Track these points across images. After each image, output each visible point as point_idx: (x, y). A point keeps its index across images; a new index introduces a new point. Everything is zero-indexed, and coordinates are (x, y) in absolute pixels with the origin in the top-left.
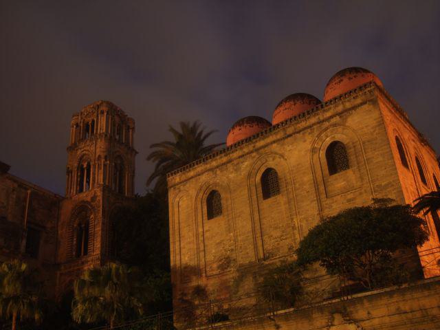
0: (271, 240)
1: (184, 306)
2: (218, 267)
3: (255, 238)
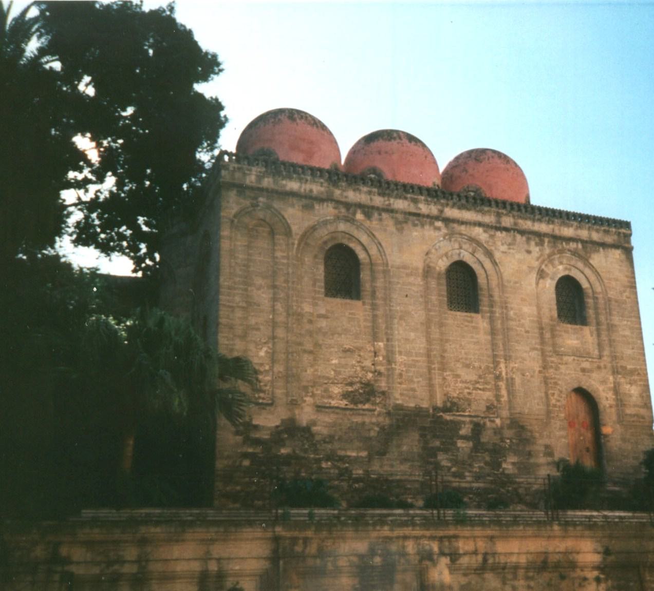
0: (456, 382)
1: (250, 450)
2: (345, 396)
3: (430, 370)
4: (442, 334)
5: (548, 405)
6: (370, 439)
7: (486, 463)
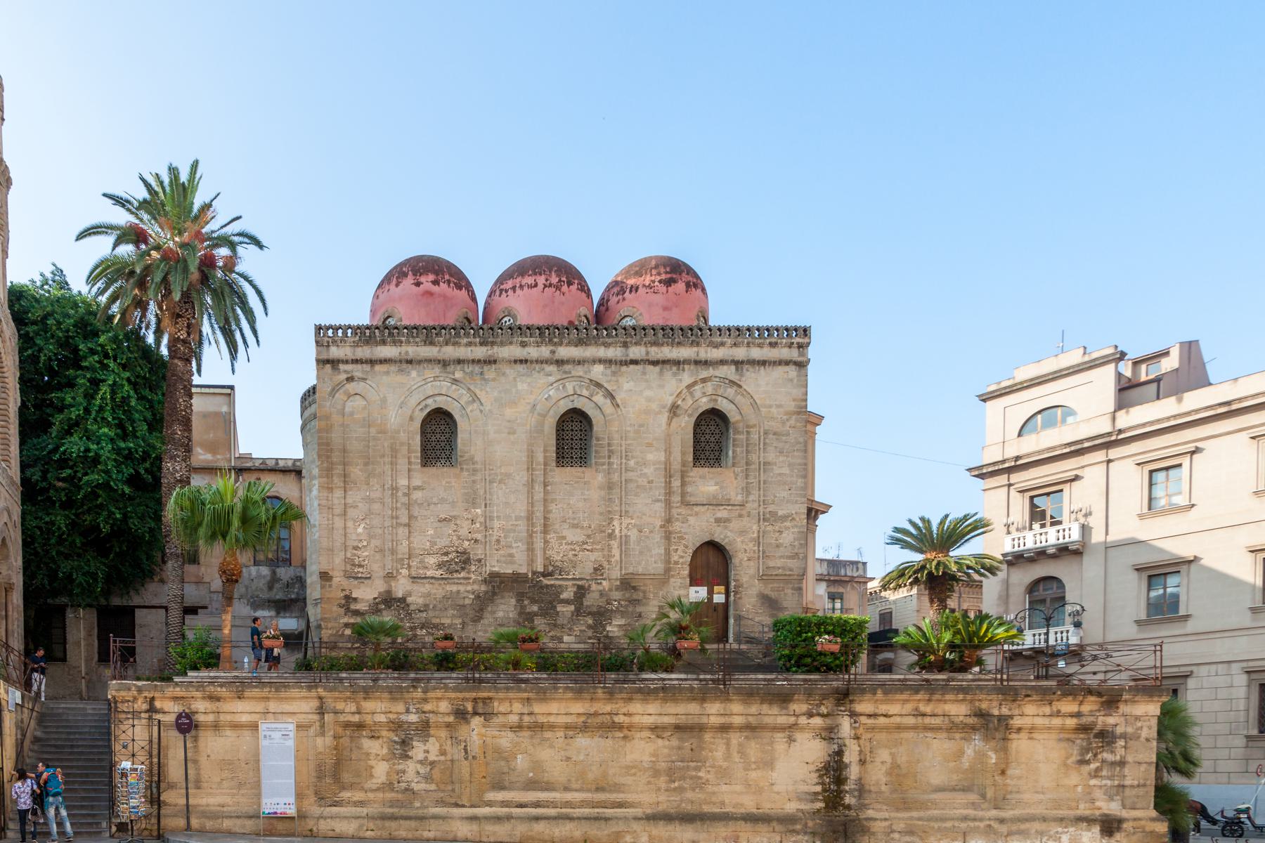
1: (352, 621)
2: (440, 566)
4: (546, 492)
5: (668, 561)
6: (464, 606)
7: (590, 627)
